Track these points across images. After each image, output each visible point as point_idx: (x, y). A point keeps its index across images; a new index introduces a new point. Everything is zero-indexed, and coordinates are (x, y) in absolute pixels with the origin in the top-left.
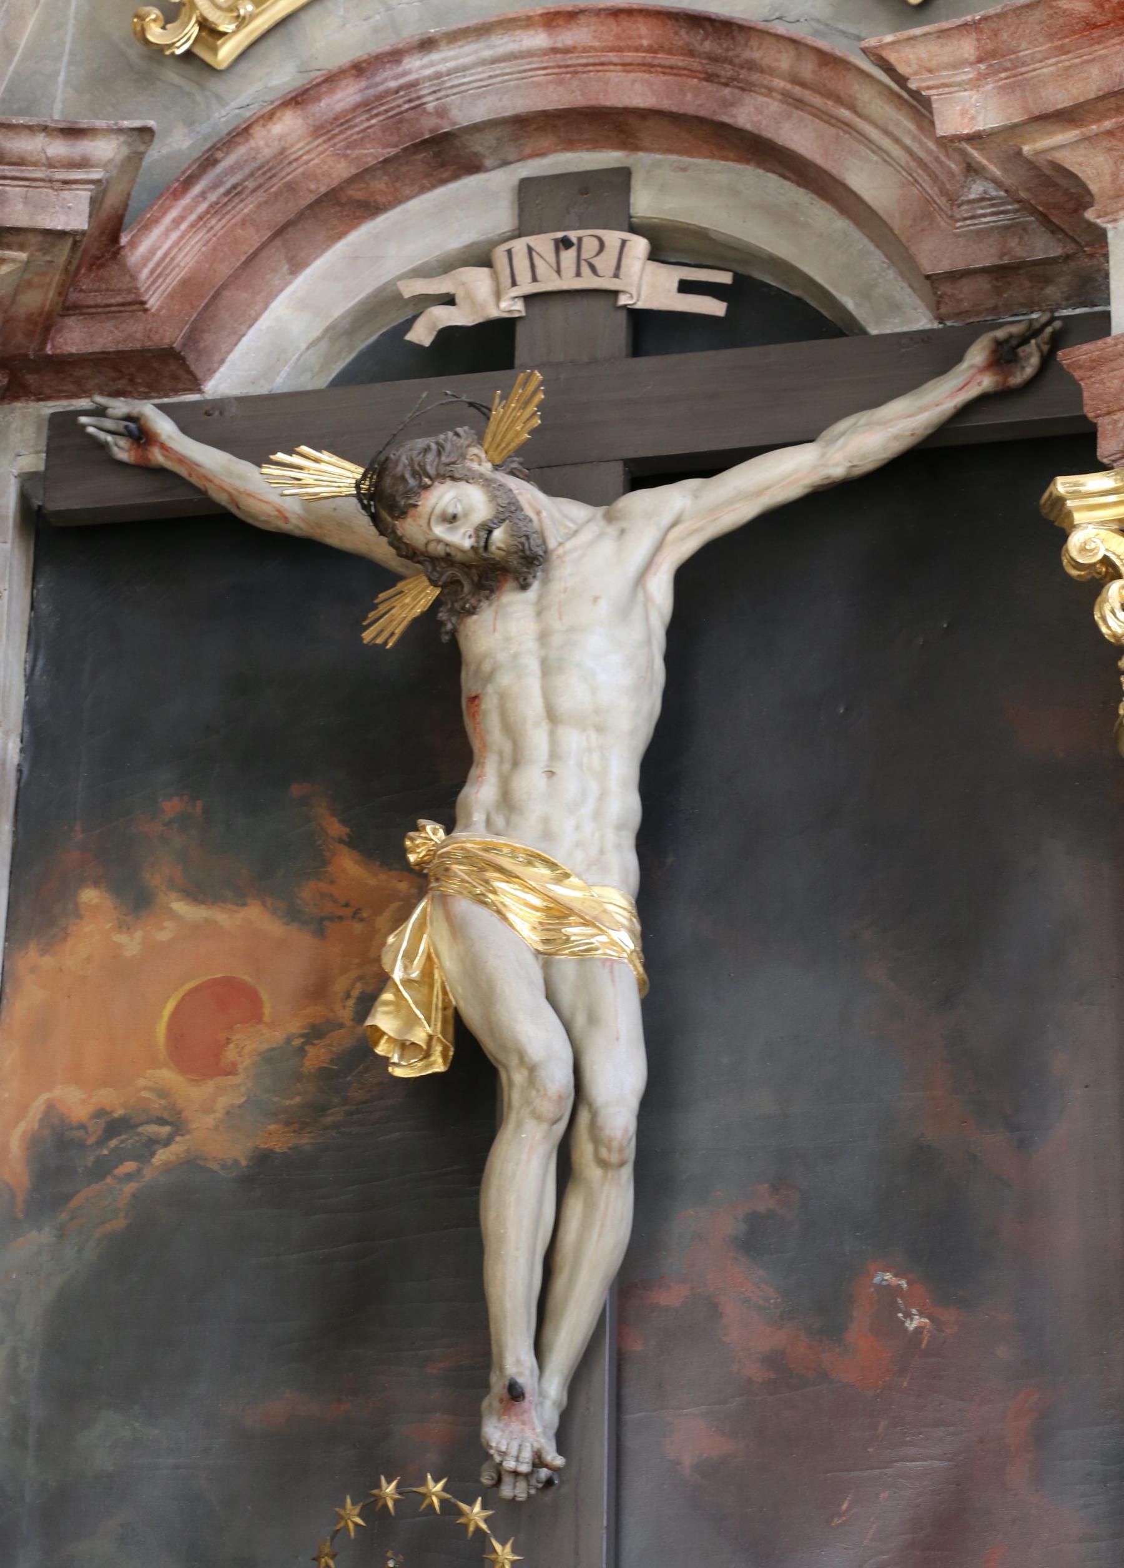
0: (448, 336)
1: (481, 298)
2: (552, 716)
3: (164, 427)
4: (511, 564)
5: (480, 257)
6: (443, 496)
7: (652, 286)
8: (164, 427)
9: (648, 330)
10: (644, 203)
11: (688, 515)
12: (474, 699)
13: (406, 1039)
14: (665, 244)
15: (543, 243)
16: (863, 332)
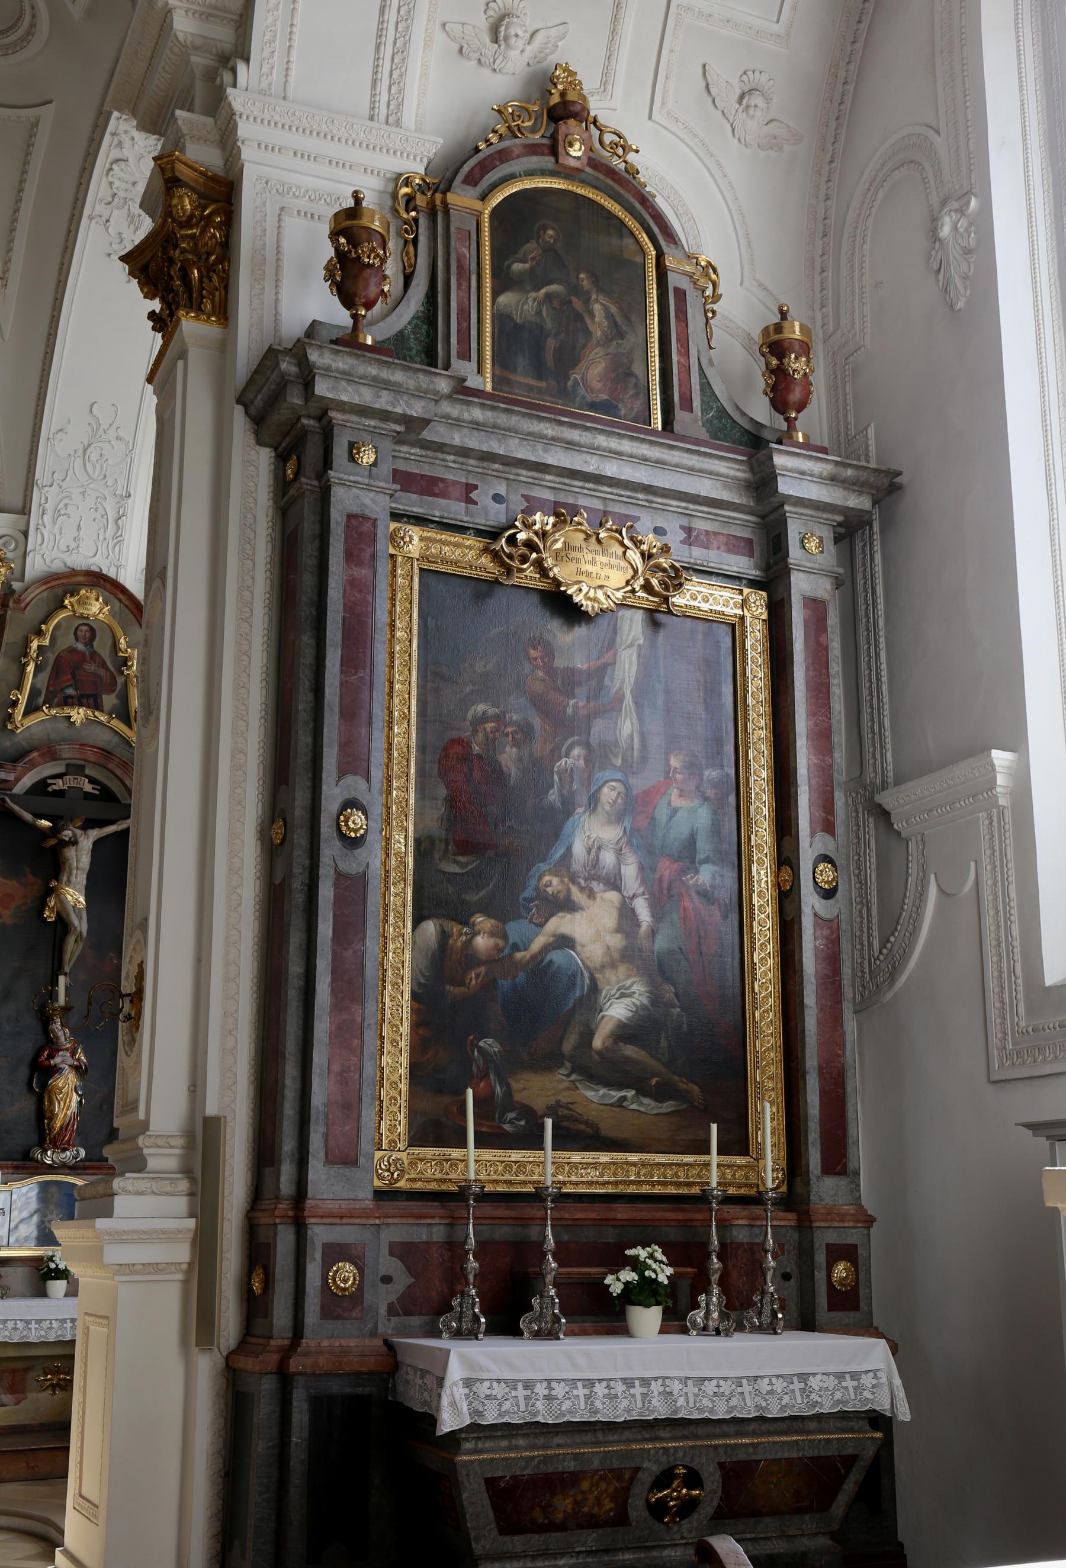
0: (54, 791)
1: (59, 785)
2: (77, 868)
3: (8, 800)
4: (74, 842)
5: (60, 776)
6: (66, 832)
7: (88, 787)
8: (8, 800)
9: (87, 796)
10: (87, 772)
11: (95, 834)
12: (64, 863)
13: (49, 915)
14: (92, 781)
15: (72, 777)
16: (119, 801)
